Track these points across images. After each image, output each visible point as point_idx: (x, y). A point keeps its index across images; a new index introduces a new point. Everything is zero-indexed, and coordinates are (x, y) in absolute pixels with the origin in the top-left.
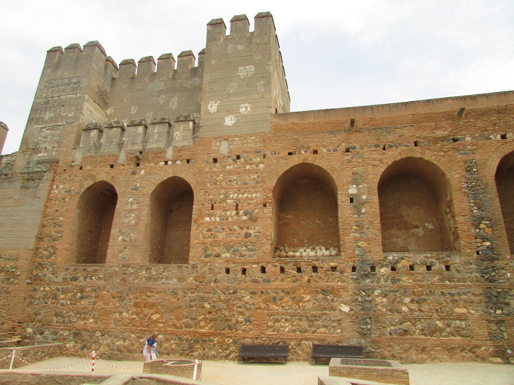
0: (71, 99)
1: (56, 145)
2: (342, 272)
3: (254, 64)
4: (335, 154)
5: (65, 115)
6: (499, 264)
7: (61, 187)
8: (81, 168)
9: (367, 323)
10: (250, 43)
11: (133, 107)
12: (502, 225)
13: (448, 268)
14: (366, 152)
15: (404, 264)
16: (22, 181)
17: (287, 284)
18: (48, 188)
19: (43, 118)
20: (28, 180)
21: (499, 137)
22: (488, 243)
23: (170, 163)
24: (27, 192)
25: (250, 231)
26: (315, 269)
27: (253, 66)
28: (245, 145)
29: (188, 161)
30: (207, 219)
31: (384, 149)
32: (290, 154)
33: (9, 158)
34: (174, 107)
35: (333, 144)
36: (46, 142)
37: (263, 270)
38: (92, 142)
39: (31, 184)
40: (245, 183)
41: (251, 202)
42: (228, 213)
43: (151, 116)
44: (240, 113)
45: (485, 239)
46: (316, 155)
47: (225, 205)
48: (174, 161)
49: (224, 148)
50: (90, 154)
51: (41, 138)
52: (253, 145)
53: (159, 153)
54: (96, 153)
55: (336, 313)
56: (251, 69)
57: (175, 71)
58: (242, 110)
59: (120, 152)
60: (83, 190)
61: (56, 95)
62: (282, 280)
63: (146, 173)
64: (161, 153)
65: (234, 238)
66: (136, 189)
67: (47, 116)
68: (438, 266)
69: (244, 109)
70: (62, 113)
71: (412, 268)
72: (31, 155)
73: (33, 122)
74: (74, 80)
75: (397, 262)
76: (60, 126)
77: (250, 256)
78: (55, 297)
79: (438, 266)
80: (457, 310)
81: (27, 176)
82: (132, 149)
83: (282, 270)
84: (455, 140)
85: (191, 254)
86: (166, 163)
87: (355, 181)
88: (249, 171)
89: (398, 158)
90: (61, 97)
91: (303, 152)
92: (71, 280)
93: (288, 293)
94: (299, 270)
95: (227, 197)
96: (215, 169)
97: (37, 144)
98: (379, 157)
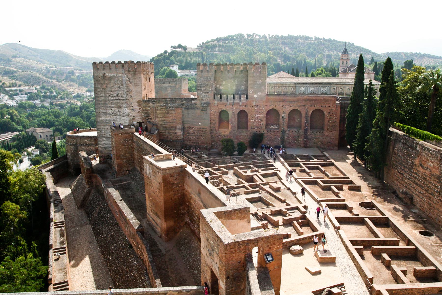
0: (209, 84)
5: (208, 89)
12: (310, 124)
17: (269, 134)
26: (274, 131)
37: (264, 131)
39: (203, 109)
49: (254, 103)
50: (219, 102)
53: (238, 104)
56: (261, 81)
58: (259, 93)
67: (203, 89)
72: (201, 101)
78: (218, 137)
83: (268, 132)
87: (284, 113)
94: (271, 131)
95: (255, 115)
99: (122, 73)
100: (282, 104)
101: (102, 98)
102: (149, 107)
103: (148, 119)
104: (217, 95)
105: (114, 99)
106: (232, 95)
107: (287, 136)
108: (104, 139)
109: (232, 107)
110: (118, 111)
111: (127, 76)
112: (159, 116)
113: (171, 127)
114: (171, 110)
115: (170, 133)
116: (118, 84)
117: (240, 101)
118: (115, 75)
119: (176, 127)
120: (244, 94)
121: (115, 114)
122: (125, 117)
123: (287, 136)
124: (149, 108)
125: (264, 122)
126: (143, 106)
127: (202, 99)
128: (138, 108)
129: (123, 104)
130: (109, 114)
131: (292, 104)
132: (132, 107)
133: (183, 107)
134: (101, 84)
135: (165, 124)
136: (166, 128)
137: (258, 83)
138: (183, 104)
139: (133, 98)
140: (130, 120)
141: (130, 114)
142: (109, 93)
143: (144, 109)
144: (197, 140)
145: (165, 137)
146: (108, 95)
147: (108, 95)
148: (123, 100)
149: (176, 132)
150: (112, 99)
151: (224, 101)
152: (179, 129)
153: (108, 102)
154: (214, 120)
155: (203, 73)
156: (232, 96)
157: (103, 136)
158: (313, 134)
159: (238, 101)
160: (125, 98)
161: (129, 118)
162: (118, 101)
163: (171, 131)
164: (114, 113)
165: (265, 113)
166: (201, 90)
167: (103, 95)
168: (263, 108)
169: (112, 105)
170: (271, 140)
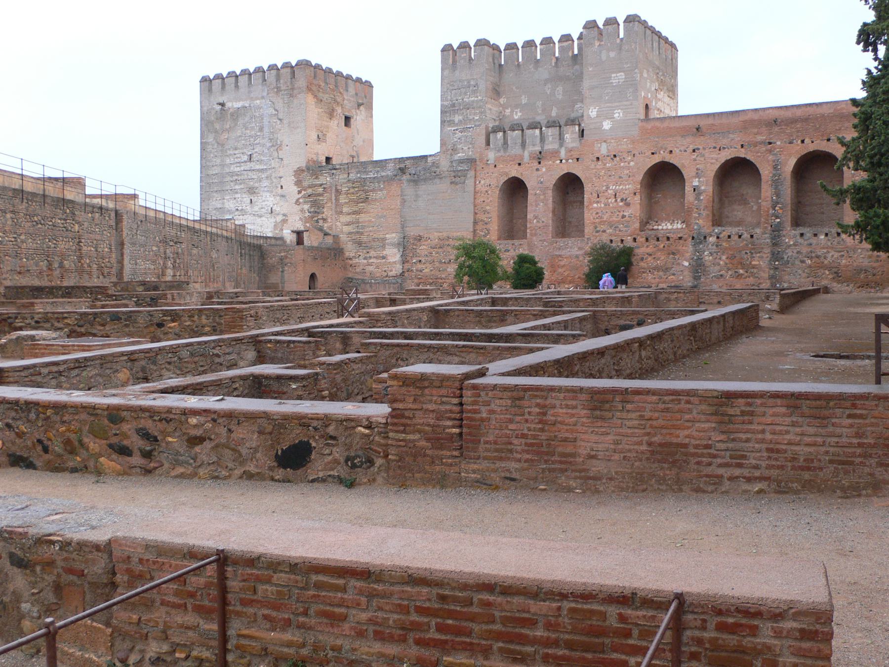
0: (473, 101)
2: (685, 241)
3: (623, 72)
4: (685, 154)
5: (471, 117)
6: (784, 233)
8: (495, 166)
9: (698, 273)
10: (620, 49)
11: (523, 96)
12: (789, 208)
13: (752, 236)
14: (706, 153)
15: (724, 235)
17: (649, 250)
18: (473, 184)
19: (454, 121)
20: (455, 177)
21: (799, 142)
22: (778, 220)
23: (564, 161)
24: (457, 187)
25: (625, 214)
26: (668, 238)
27: (623, 74)
28: (620, 147)
29: (578, 159)
30: (595, 205)
31: (720, 150)
32: (653, 154)
33: (433, 158)
34: (560, 97)
35: (683, 145)
37: (635, 240)
39: (458, 179)
40: (620, 177)
41: (626, 192)
42: (610, 200)
43: (540, 106)
44: (614, 118)
45: (777, 217)
46: (671, 155)
47: (606, 194)
48: (567, 160)
49: (604, 149)
50: (500, 154)
52: (625, 147)
53: (555, 154)
55: (681, 266)
56: (621, 76)
57: (557, 58)
58: (616, 115)
59: (524, 152)
60: (500, 185)
62: (647, 247)
63: (547, 170)
64: (556, 153)
65: (614, 219)
66: (542, 183)
67: (457, 118)
68: (746, 236)
69: (618, 114)
71: (729, 237)
72: (451, 155)
73: (446, 124)
74: (472, 83)
75: (720, 233)
77: (626, 231)
79: (746, 236)
80: (753, 263)
81: (453, 174)
82: (533, 149)
83: (647, 240)
84: (770, 143)
85: (586, 231)
86: (561, 161)
87: (698, 175)
88: (623, 167)
89: (729, 158)
91: (662, 152)
92: (505, 251)
93: (650, 255)
94: (658, 239)
95: (608, 188)
96: (598, 167)
98: (716, 156)
99: (263, 97)
100: (689, 142)
101: (216, 170)
102: (321, 185)
103: (317, 221)
104: (495, 130)
105: (242, 168)
106: (536, 128)
107: (711, 254)
109: (539, 166)
110: (249, 201)
111: (273, 103)
112: (345, 210)
113: (374, 240)
114: (373, 190)
115: (370, 257)
116: (252, 128)
117: (561, 145)
119: (384, 239)
120: (572, 122)
121: (243, 212)
122: (263, 218)
123: (711, 254)
124: (321, 190)
125: (636, 209)
126: (306, 184)
128: (295, 189)
129: (260, 181)
131: (724, 142)
132: (282, 186)
133: (405, 177)
134: (216, 132)
135: (358, 232)
136: (360, 244)
137: (614, 82)
138: (402, 170)
139: (285, 162)
140: (275, 226)
141: (277, 209)
142: (230, 155)
143: (310, 191)
144: (437, 273)
145: (358, 270)
146: (228, 161)
147: (228, 161)
148: (262, 171)
149: (384, 252)
151: (515, 150)
152: (392, 244)
153: (228, 179)
154: (485, 212)
155: (457, 73)
156: (537, 132)
158: (800, 240)
159: (556, 146)
160: (266, 164)
161: (273, 220)
162: (250, 173)
163: (372, 253)
164: (240, 208)
165: (640, 177)
166: (451, 123)
167: (218, 161)
168: (632, 164)
170: (657, 268)
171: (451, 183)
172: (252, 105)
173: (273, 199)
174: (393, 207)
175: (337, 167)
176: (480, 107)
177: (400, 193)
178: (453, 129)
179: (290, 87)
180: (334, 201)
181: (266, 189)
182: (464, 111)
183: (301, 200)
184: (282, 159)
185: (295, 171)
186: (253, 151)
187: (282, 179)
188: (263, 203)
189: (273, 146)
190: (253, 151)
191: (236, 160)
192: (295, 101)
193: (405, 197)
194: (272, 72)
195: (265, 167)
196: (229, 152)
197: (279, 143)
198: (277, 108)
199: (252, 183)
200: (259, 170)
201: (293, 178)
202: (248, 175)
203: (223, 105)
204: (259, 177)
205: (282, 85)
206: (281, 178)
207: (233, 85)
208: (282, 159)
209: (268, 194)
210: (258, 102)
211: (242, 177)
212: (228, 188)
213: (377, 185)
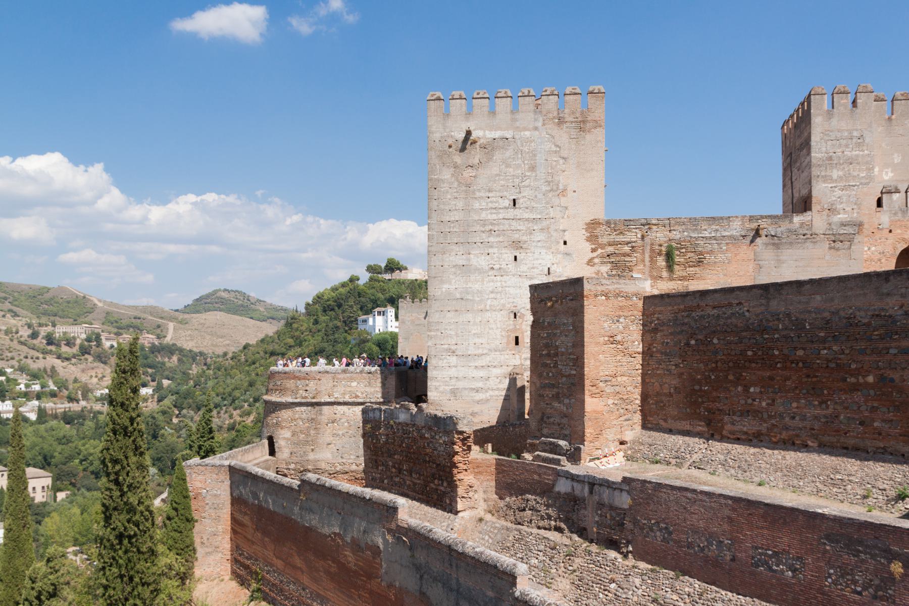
0: (857, 156)
1: (855, 207)
5: (855, 174)
7: (873, 248)
11: (896, 155)
16: (828, 242)
19: (831, 176)
20: (834, 241)
36: (842, 203)
38: (897, 207)
51: (834, 199)
54: (904, 217)
61: (839, 150)
67: (835, 174)
70: (851, 172)
72: (828, 216)
73: (820, 179)
74: (855, 134)
76: (853, 186)
90: (845, 153)
97: (832, 204)
99: (536, 129)
105: (501, 216)
108: (453, 360)
111: (553, 137)
114: (711, 252)
116: (518, 166)
118: (509, 134)
121: (502, 272)
124: (627, 249)
126: (604, 240)
127: (832, 210)
128: (588, 246)
129: (531, 234)
130: (479, 271)
132: (565, 243)
142: (481, 198)
143: (610, 249)
147: (477, 205)
150: (494, 216)
153: (478, 228)
155: (834, 122)
157: (449, 350)
160: (541, 213)
162: (514, 223)
166: (827, 179)
167: (460, 204)
169: (491, 239)
171: (830, 248)
172: (517, 137)
173: (551, 256)
174: (741, 273)
175: (654, 222)
176: (867, 163)
177: (752, 257)
178: (830, 185)
179: (580, 119)
180: (647, 263)
181: (539, 244)
182: (845, 166)
183: (596, 261)
184: (566, 208)
185: (587, 224)
186: (520, 196)
187: (566, 233)
188: (535, 262)
189: (552, 190)
190: (520, 196)
191: (490, 205)
192: (588, 137)
193: (760, 262)
194: (551, 97)
195: (539, 217)
196: (478, 194)
197: (561, 187)
198: (559, 143)
199: (517, 236)
200: (527, 220)
201: (584, 232)
202: (510, 225)
203: (469, 133)
204: (529, 228)
205: (566, 116)
206: (564, 231)
207: (486, 109)
208: (566, 208)
209: (543, 251)
210: (527, 133)
211: (501, 227)
212: (478, 239)
213: (716, 246)
